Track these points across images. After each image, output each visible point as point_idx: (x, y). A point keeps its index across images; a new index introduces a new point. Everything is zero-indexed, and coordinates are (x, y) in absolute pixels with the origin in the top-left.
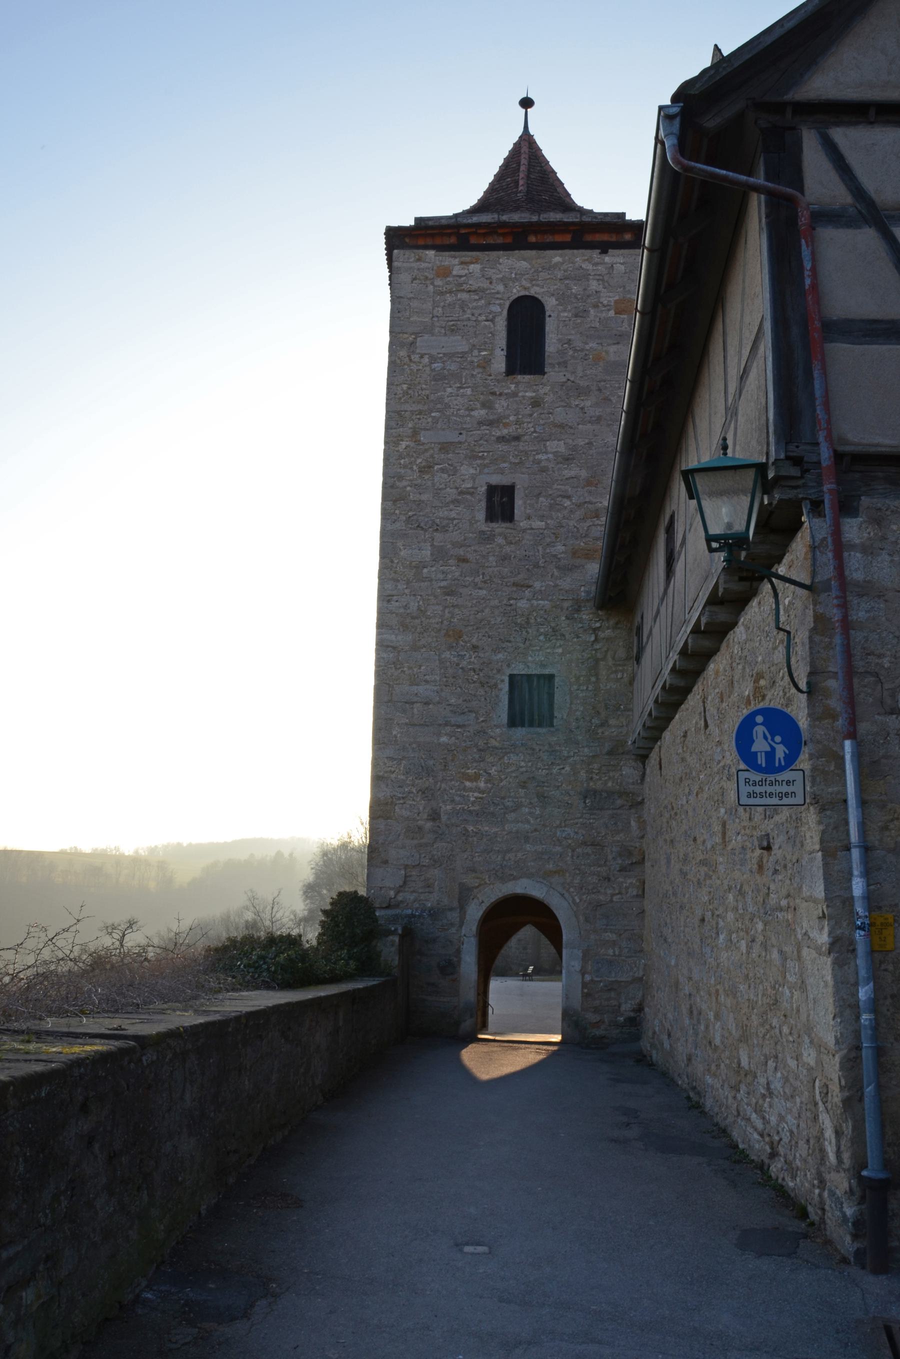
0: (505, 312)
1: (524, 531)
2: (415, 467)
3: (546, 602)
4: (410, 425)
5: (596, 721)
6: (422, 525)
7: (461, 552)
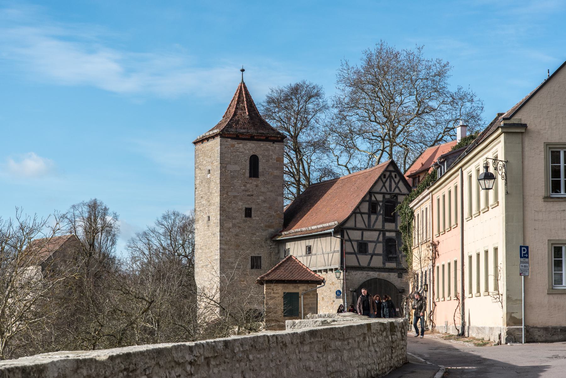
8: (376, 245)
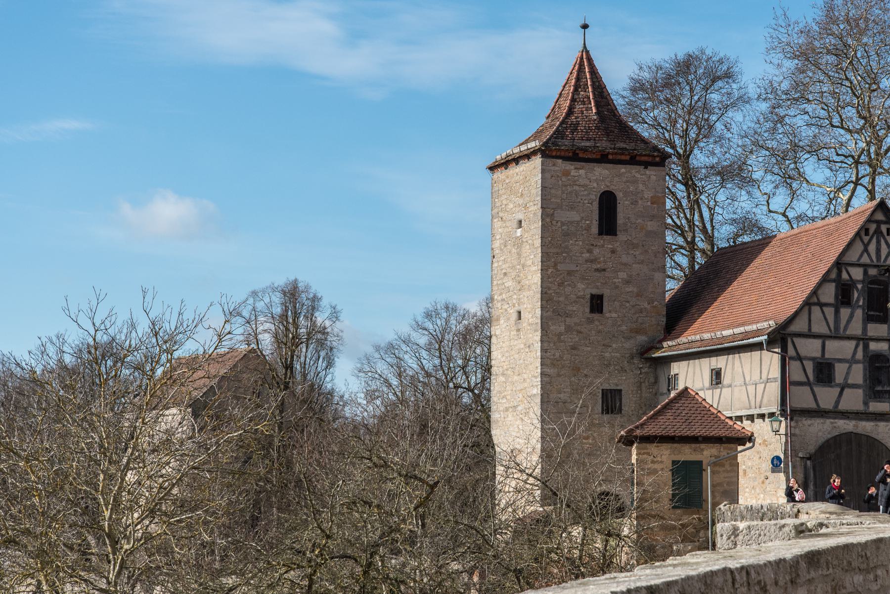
5: (641, 412)
7: (579, 328)
8: (850, 367)
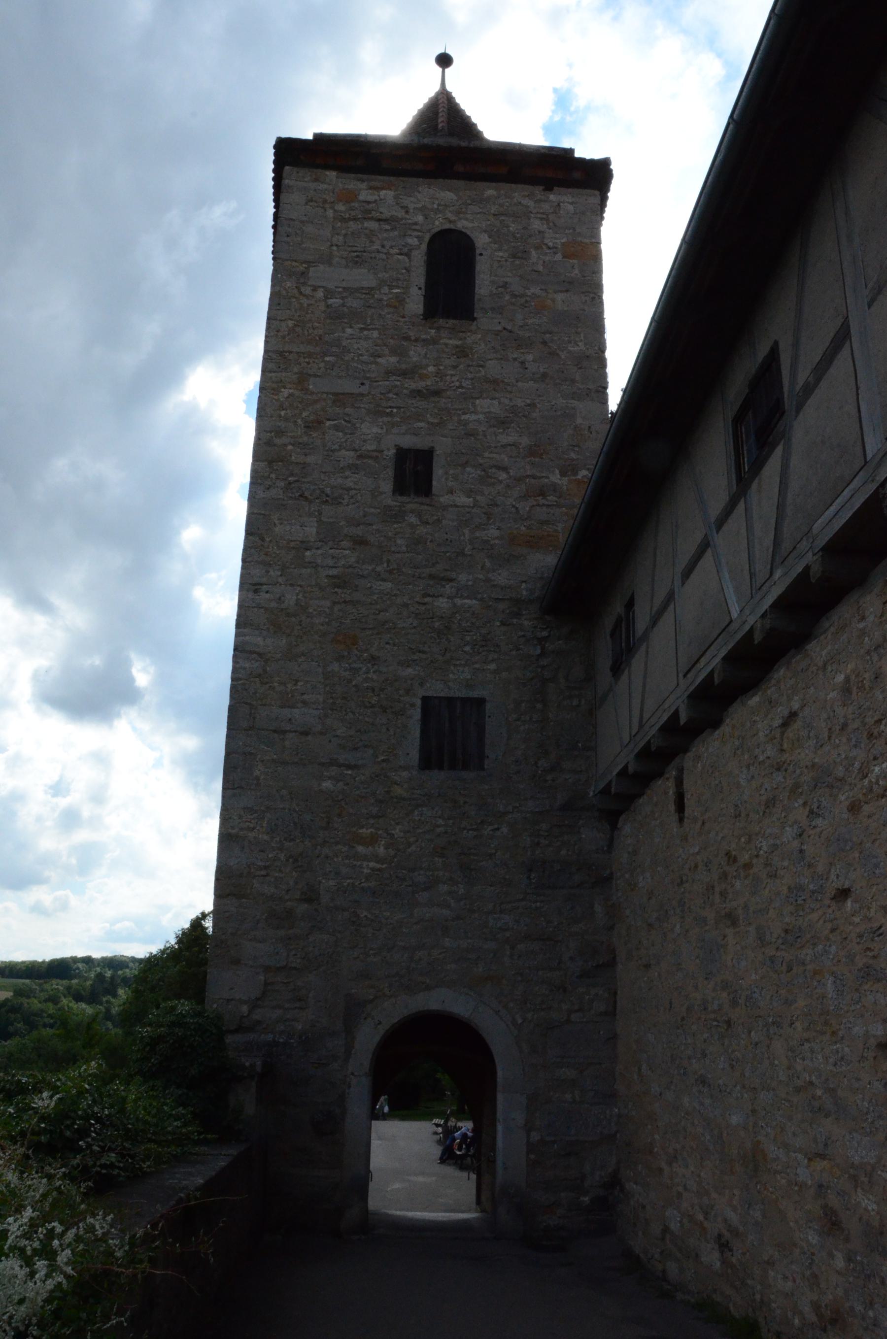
0: (424, 247)
1: (445, 508)
2: (299, 421)
3: (474, 601)
4: (296, 370)
6: (306, 494)
7: (359, 531)
